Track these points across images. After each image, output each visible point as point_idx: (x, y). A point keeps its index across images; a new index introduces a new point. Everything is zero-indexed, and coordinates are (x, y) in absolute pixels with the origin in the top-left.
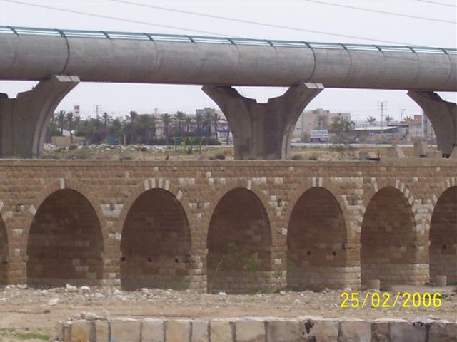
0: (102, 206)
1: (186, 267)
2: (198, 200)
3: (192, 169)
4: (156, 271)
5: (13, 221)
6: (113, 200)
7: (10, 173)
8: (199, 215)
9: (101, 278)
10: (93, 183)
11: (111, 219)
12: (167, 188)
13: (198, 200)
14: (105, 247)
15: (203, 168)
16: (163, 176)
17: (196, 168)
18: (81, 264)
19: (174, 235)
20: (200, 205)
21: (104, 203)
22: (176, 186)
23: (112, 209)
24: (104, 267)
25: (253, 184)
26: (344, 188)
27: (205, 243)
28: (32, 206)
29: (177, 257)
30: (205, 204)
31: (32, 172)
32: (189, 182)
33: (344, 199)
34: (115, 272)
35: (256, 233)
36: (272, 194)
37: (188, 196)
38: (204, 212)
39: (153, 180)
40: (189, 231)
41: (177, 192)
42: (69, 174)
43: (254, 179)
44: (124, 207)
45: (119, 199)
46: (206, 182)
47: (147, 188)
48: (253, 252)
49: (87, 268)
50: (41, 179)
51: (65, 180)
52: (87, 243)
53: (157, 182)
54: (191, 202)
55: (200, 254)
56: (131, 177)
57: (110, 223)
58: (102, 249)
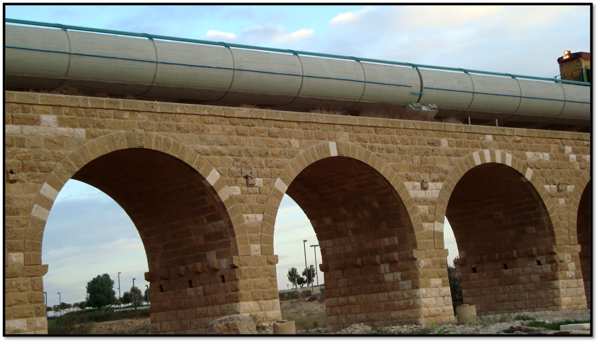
0: (406, 183)
1: (552, 269)
2: (557, 181)
3: (544, 140)
4: (514, 281)
5: (242, 201)
6: (425, 176)
7: (229, 128)
8: (562, 201)
9: (417, 288)
10: (389, 152)
11: (424, 201)
12: (509, 163)
13: (557, 181)
14: (418, 241)
15: (559, 141)
16: (500, 147)
17: (550, 140)
18: (392, 271)
19: (532, 229)
21: (409, 179)
22: (523, 162)
23: (424, 188)
24: (420, 270)
27: (574, 237)
28: (278, 180)
29: (539, 258)
30: (569, 187)
31: (275, 130)
32: (542, 158)
34: (440, 277)
37: (542, 176)
38: (568, 197)
39: (487, 152)
40: (550, 221)
41: (525, 169)
42: (344, 136)
44: (445, 187)
45: (436, 176)
46: (567, 159)
47: (478, 162)
49: (398, 275)
50: (293, 141)
51: (337, 144)
52: (396, 240)
53: (493, 155)
54: (547, 183)
55: (569, 251)
56: (450, 146)
58: (415, 246)
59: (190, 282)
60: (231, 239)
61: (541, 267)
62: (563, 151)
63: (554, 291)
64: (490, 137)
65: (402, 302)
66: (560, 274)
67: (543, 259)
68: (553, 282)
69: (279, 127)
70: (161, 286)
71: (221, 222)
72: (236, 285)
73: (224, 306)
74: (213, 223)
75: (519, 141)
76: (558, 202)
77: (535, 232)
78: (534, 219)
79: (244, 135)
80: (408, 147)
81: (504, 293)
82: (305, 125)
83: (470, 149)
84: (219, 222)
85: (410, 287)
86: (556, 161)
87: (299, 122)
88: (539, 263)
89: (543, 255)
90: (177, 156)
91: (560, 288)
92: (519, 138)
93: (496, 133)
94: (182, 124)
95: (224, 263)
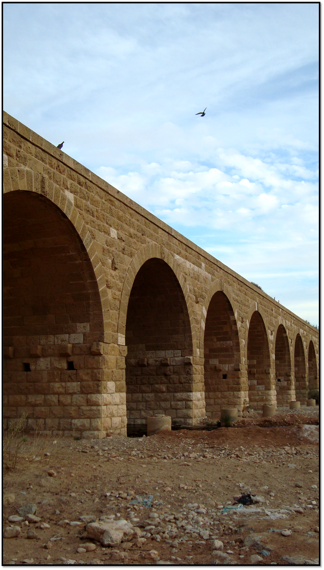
9: (269, 390)
60: (235, 353)
61: (281, 383)
63: (288, 396)
65: (257, 397)
68: (288, 391)
72: (239, 381)
73: (225, 393)
74: (222, 342)
77: (278, 363)
78: (280, 356)
84: (228, 342)
85: (264, 389)
89: (282, 376)
91: (292, 394)
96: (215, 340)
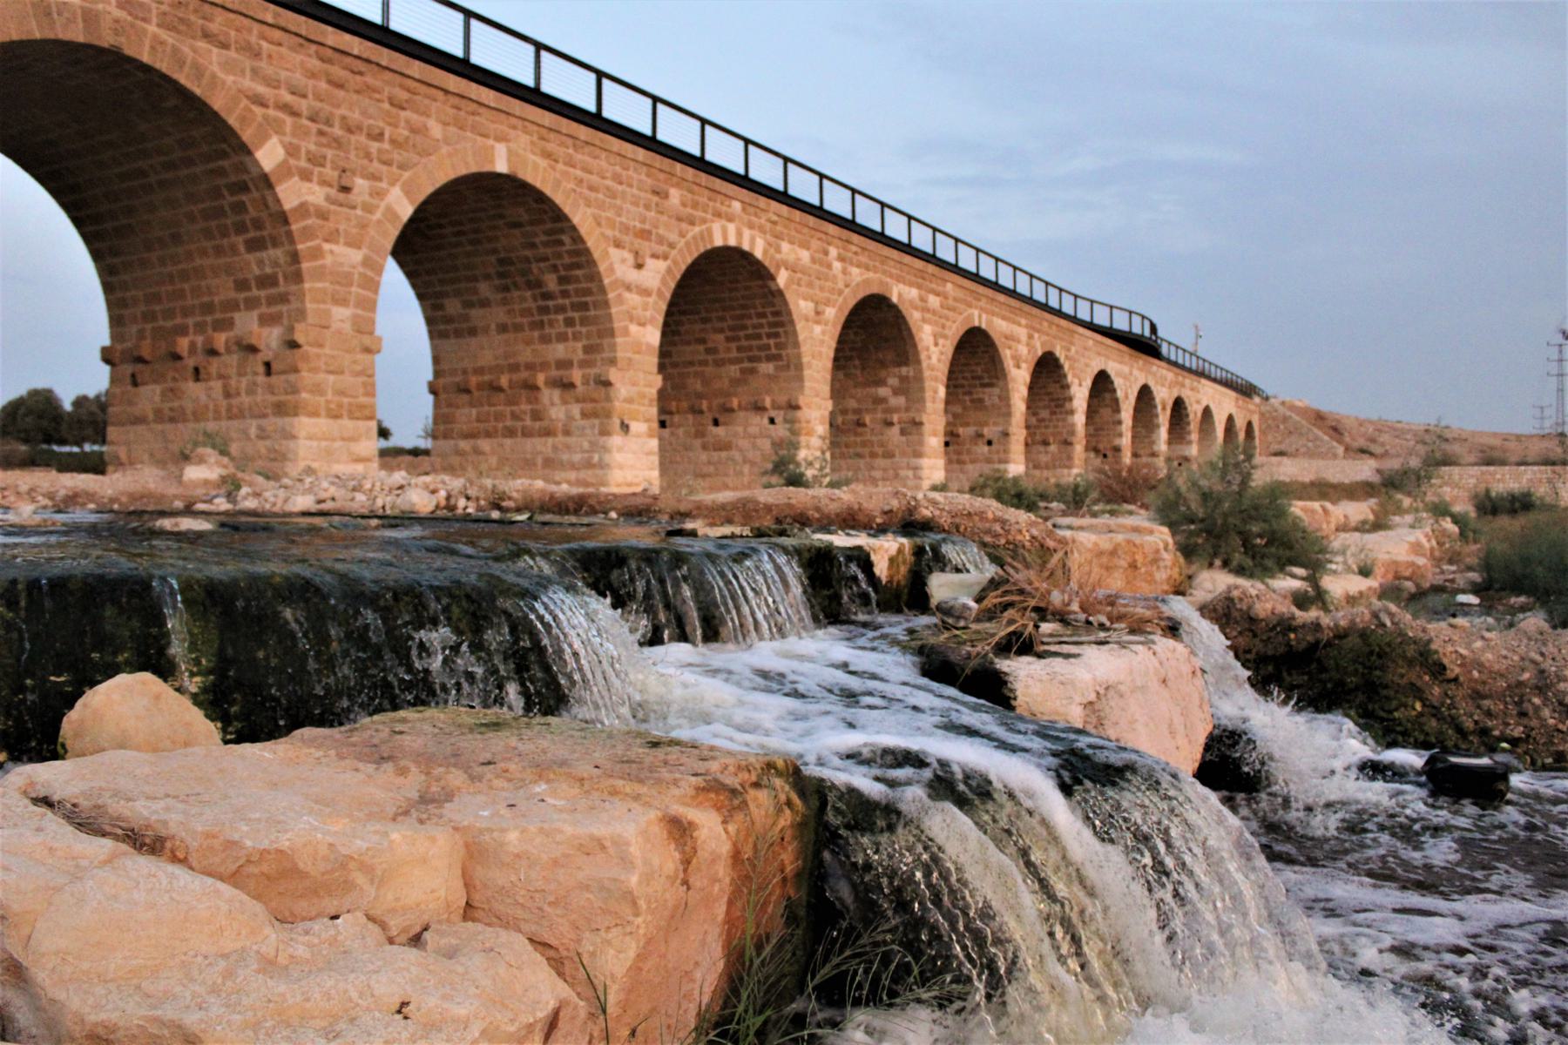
0: (613, 251)
3: (806, 230)
4: (724, 446)
7: (314, 63)
8: (818, 329)
14: (619, 355)
16: (751, 226)
19: (767, 368)
20: (821, 308)
21: (618, 245)
24: (617, 404)
25: (900, 295)
26: (1009, 337)
31: (404, 95)
33: (1007, 355)
35: (896, 392)
36: (924, 320)
39: (731, 227)
43: (901, 286)
44: (669, 271)
46: (829, 266)
47: (719, 242)
48: (890, 424)
51: (510, 152)
53: (739, 234)
56: (684, 205)
57: (633, 299)
59: (197, 370)
62: (826, 253)
64: (737, 205)
66: (803, 439)
67: (779, 416)
69: (409, 91)
70: (133, 376)
71: (278, 254)
75: (774, 223)
76: (812, 331)
79: (340, 86)
80: (620, 188)
81: (709, 463)
82: (456, 101)
83: (709, 216)
86: (817, 267)
87: (446, 92)
88: (772, 421)
90: (198, 91)
92: (775, 218)
93: (747, 200)
94: (214, 27)
95: (270, 339)
96: (242, 248)
